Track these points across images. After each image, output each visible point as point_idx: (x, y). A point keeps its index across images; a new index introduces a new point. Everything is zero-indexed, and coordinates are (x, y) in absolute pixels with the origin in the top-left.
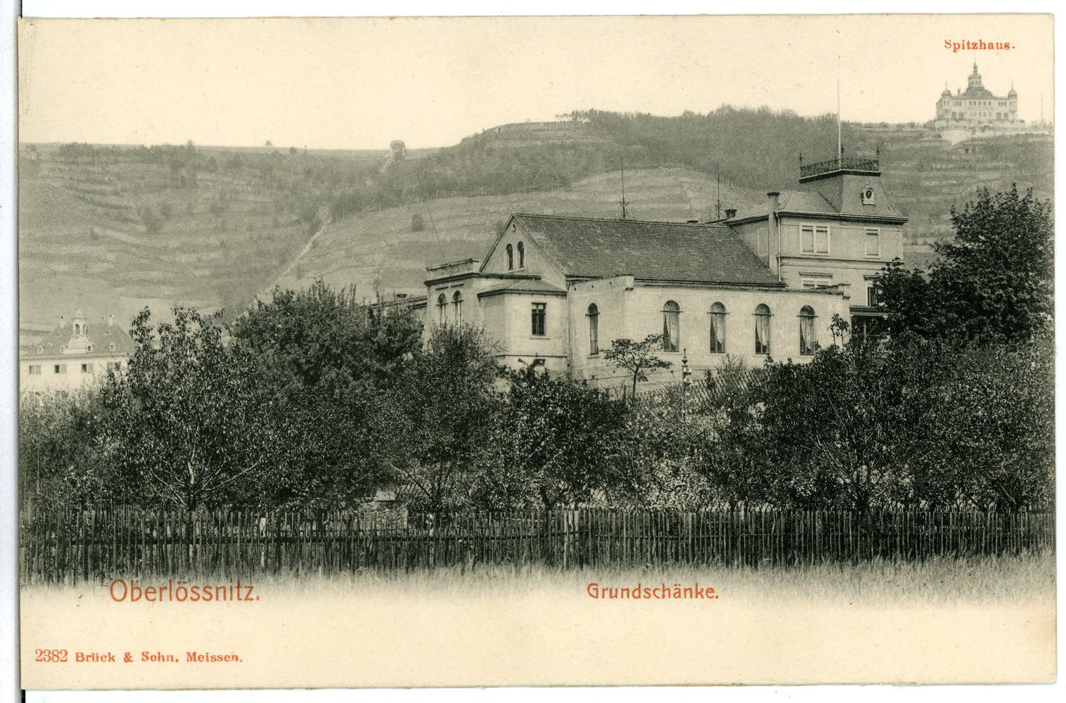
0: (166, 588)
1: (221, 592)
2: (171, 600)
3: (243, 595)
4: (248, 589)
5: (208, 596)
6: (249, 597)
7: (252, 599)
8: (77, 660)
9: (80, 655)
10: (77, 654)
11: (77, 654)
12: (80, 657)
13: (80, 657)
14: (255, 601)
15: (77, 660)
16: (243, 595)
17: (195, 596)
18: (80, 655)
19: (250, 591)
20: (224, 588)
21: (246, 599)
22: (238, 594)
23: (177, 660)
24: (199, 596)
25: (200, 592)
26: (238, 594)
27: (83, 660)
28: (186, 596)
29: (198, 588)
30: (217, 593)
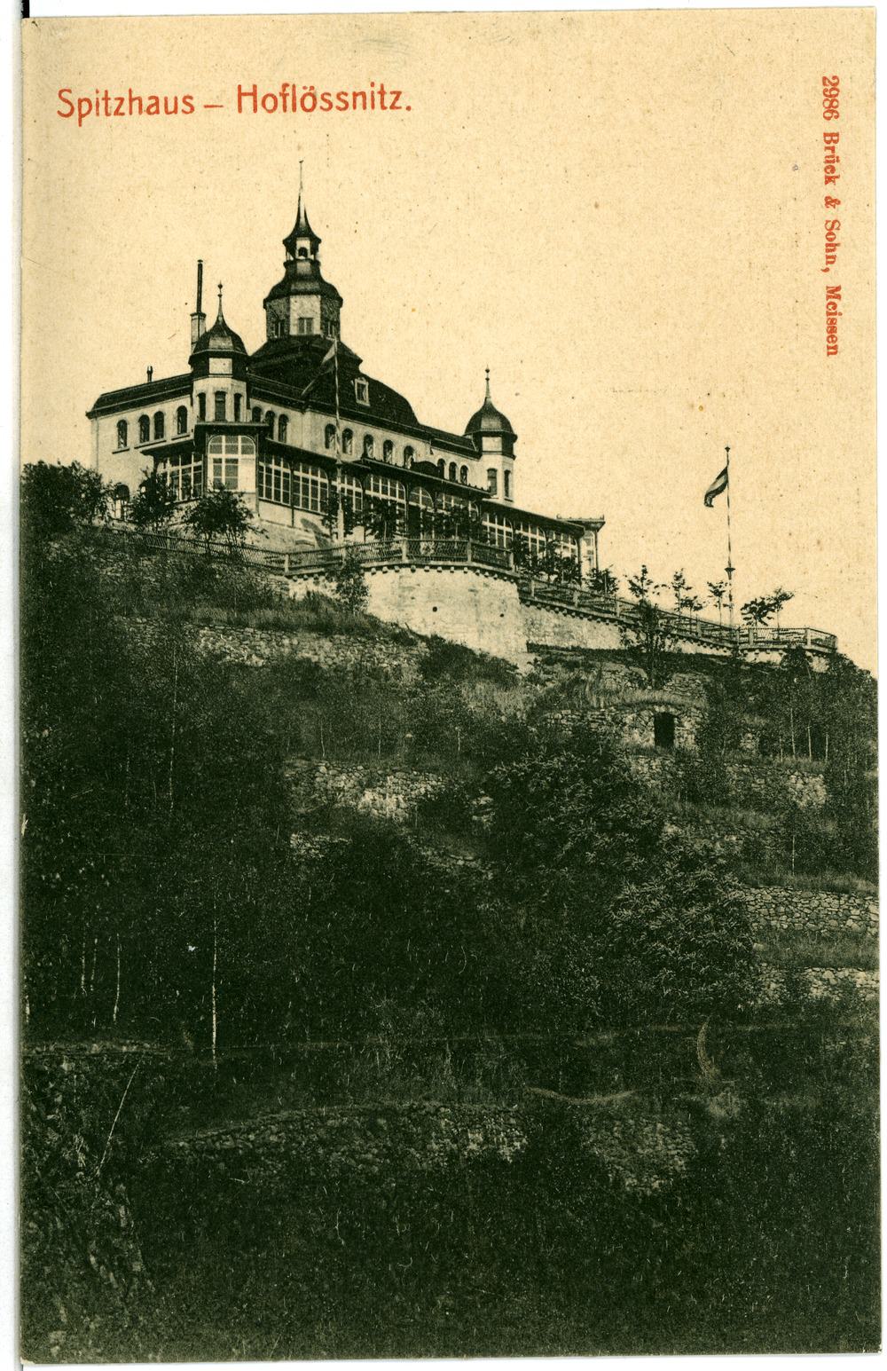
1: (360, 99)
3: (388, 103)
4: (395, 96)
5: (342, 105)
6: (397, 104)
7: (400, 108)
9: (835, 138)
11: (837, 135)
12: (831, 139)
13: (831, 139)
14: (404, 110)
16: (388, 103)
17: (326, 106)
18: (835, 138)
19: (397, 99)
20: (363, 94)
21: (393, 107)
22: (382, 100)
24: (331, 105)
25: (336, 103)
26: (382, 100)
27: (828, 142)
28: (314, 106)
29: (329, 94)
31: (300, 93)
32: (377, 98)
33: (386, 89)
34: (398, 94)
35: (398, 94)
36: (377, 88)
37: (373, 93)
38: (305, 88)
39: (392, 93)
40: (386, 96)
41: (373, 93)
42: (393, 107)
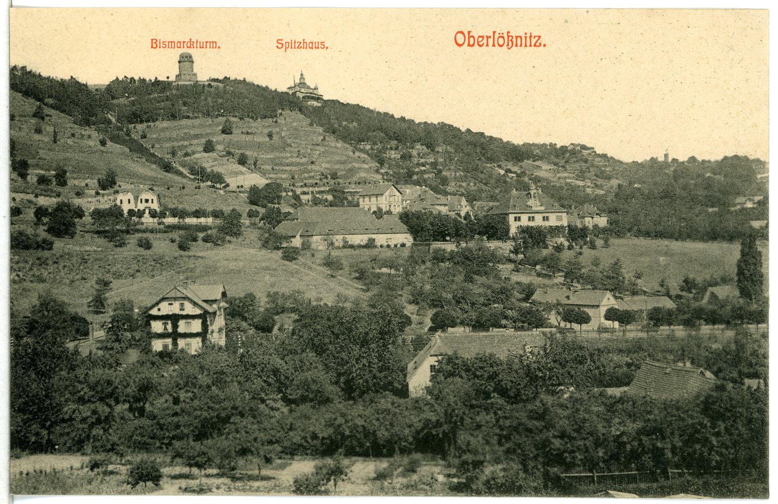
0: (490, 37)
6: (538, 44)
8: (152, 47)
10: (152, 40)
11: (152, 40)
15: (152, 47)
16: (533, 44)
20: (521, 37)
21: (535, 45)
23: (219, 47)
26: (530, 40)
30: (517, 39)
31: (497, 36)
32: (528, 39)
33: (533, 35)
34: (539, 37)
35: (539, 37)
36: (528, 35)
37: (526, 37)
38: (499, 34)
39: (535, 37)
40: (532, 38)
41: (526, 37)
42: (535, 45)
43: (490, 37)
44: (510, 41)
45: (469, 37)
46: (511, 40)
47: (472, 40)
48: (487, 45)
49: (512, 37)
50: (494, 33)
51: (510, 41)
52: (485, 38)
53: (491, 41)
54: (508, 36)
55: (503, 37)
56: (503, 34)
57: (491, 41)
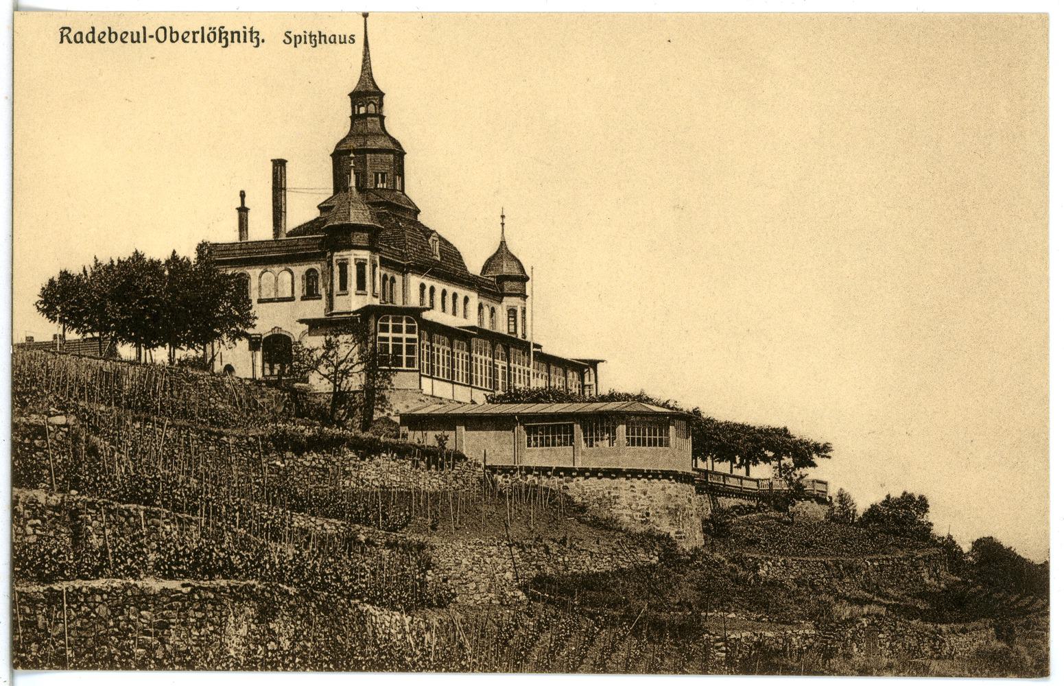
0: (198, 32)
2: (203, 41)
20: (238, 33)
26: (251, 36)
31: (207, 31)
35: (258, 33)
36: (248, 30)
37: (245, 33)
41: (245, 33)
43: (198, 32)
44: (223, 36)
45: (172, 33)
46: (225, 38)
47: (174, 36)
48: (194, 41)
49: (226, 33)
50: (203, 28)
51: (223, 36)
52: (191, 35)
53: (198, 37)
54: (221, 33)
55: (214, 33)
56: (215, 28)
57: (198, 37)
